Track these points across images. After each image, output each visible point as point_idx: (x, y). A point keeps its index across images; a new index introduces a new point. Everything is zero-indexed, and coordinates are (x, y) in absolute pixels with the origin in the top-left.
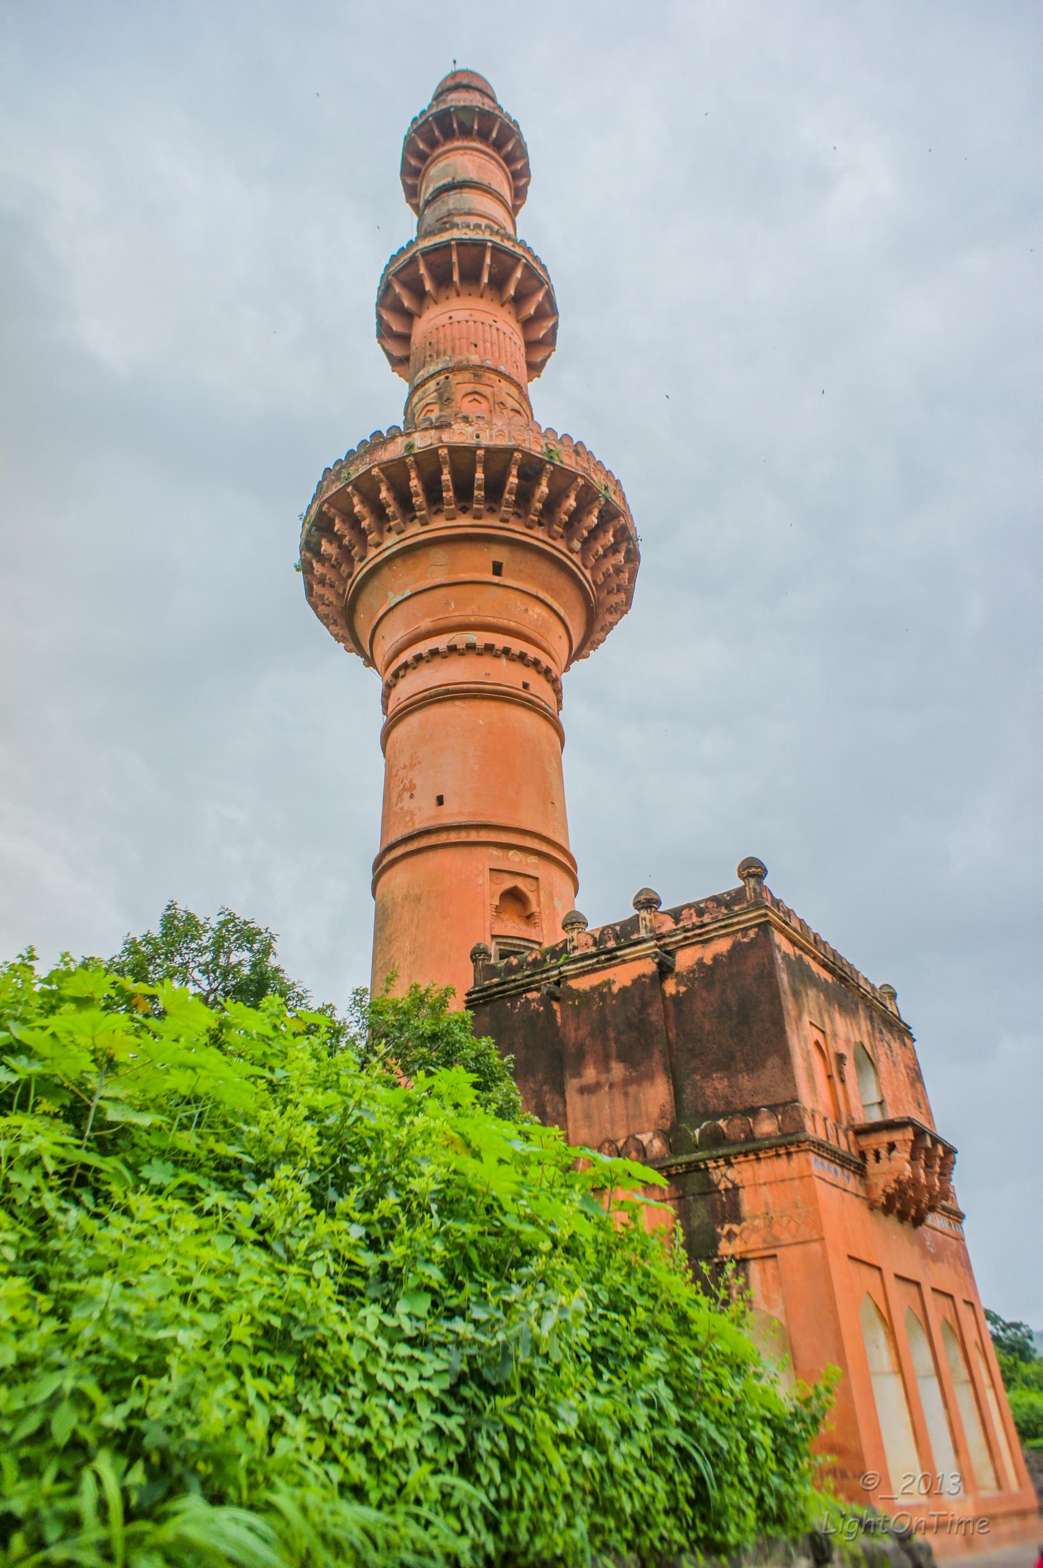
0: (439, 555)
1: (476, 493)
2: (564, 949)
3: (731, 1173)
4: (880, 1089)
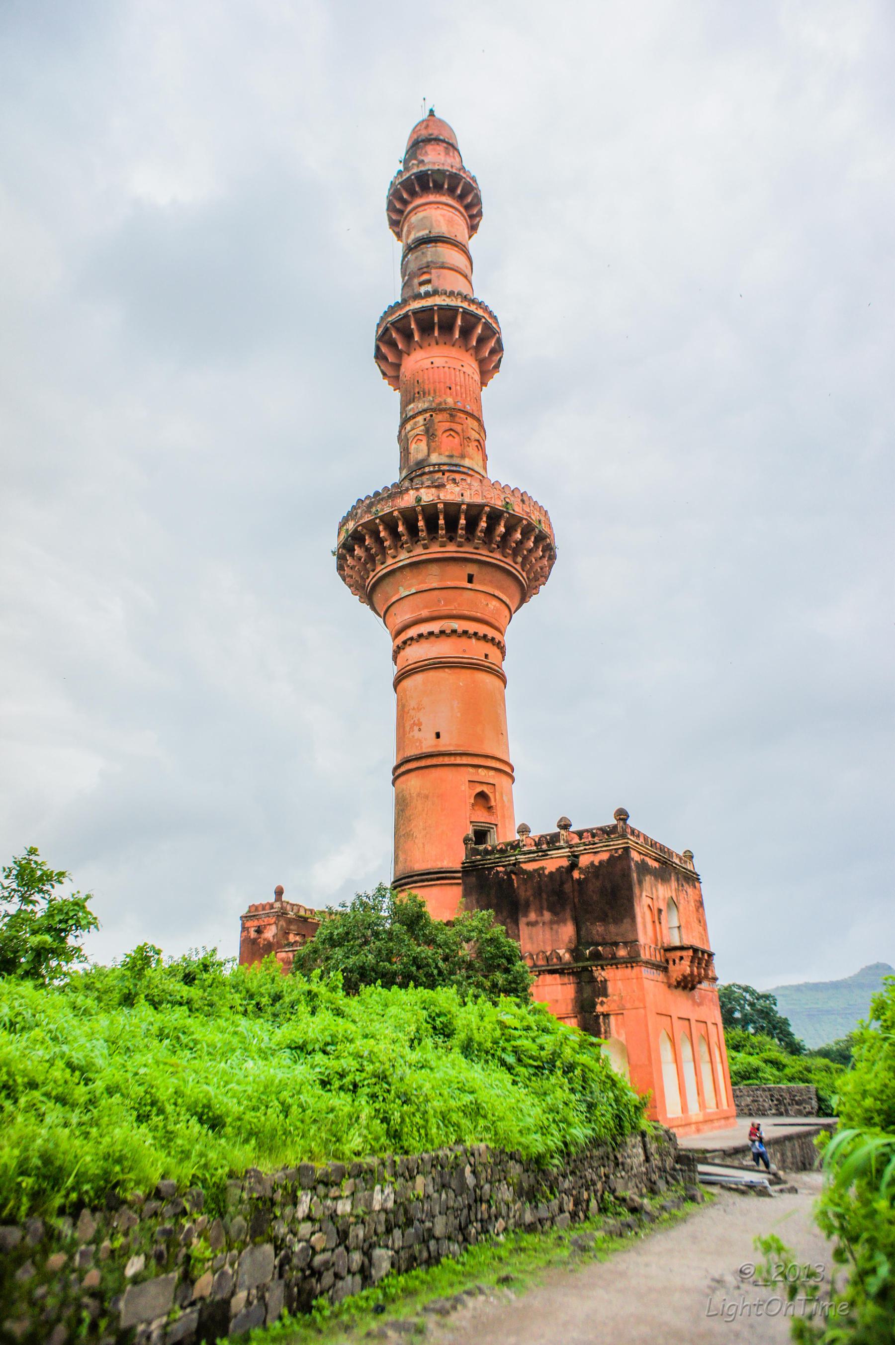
0: (434, 569)
1: (460, 532)
2: (518, 846)
3: (603, 973)
4: (679, 920)
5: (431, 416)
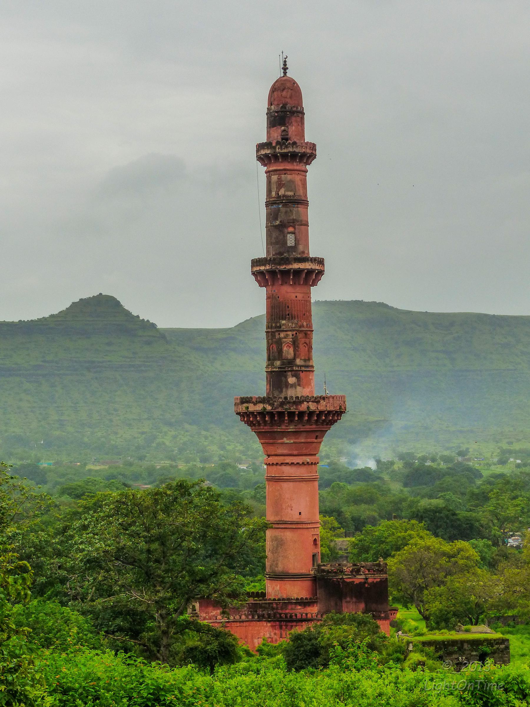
0: (304, 434)
5: (296, 333)
